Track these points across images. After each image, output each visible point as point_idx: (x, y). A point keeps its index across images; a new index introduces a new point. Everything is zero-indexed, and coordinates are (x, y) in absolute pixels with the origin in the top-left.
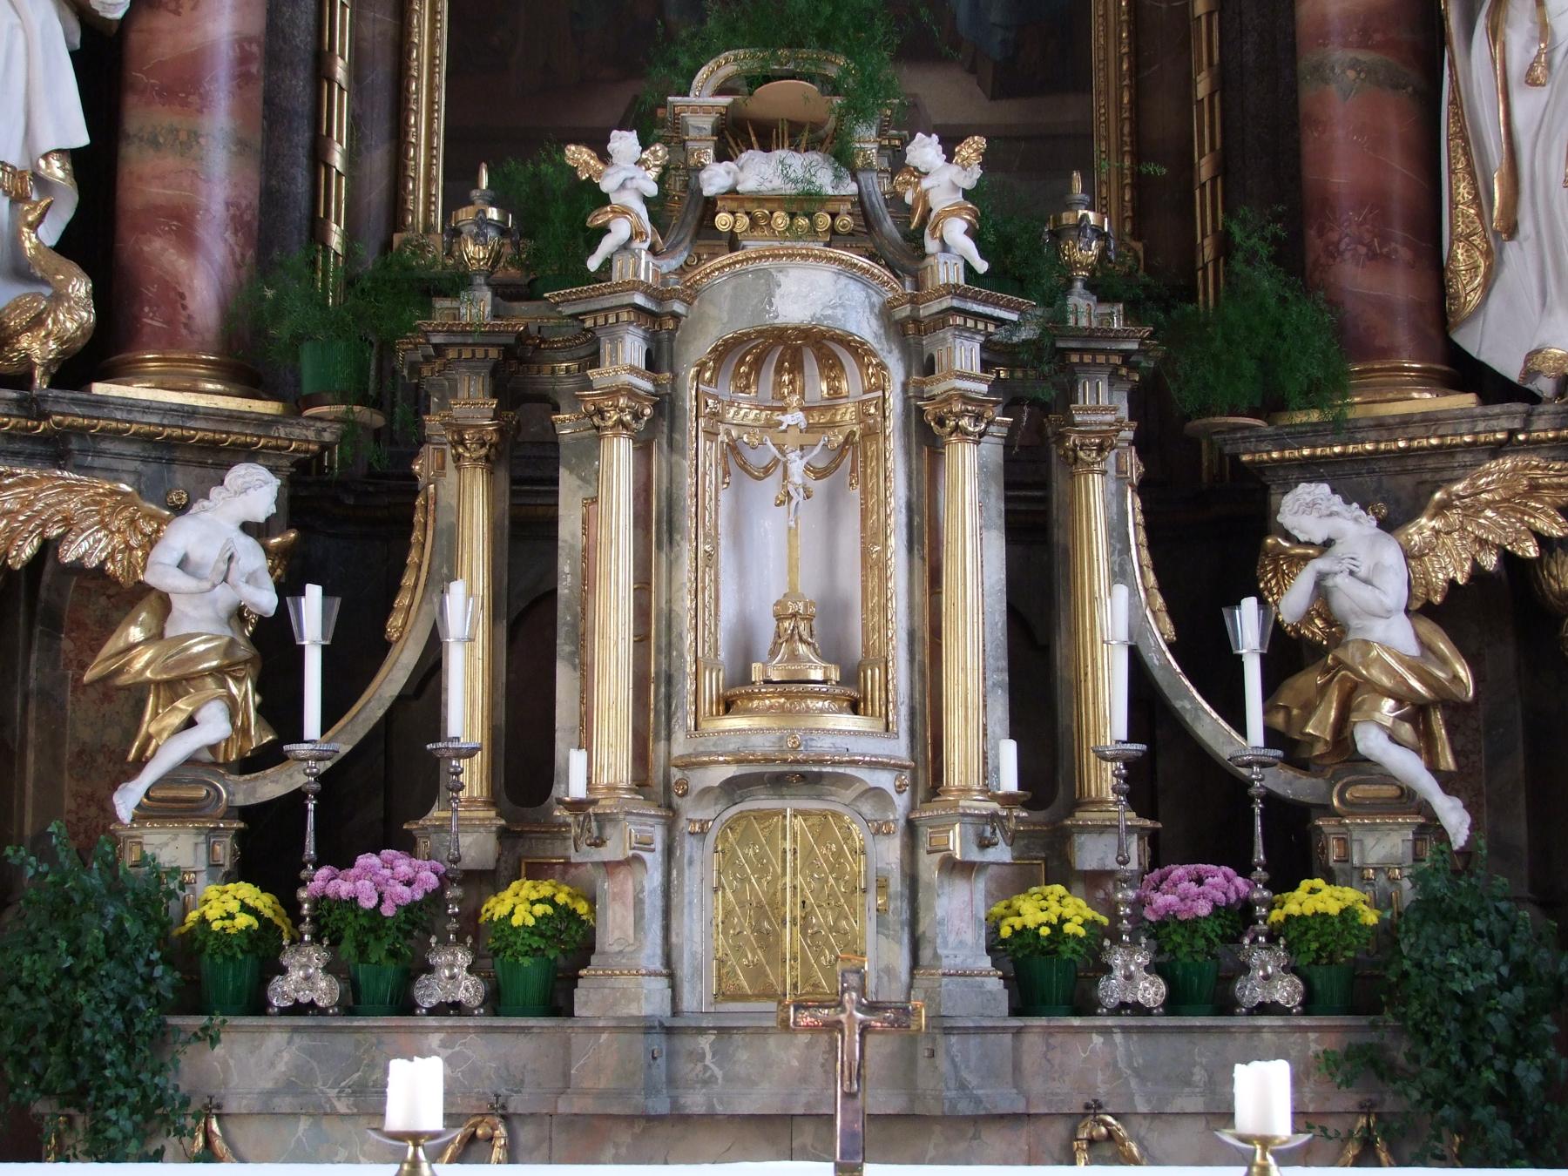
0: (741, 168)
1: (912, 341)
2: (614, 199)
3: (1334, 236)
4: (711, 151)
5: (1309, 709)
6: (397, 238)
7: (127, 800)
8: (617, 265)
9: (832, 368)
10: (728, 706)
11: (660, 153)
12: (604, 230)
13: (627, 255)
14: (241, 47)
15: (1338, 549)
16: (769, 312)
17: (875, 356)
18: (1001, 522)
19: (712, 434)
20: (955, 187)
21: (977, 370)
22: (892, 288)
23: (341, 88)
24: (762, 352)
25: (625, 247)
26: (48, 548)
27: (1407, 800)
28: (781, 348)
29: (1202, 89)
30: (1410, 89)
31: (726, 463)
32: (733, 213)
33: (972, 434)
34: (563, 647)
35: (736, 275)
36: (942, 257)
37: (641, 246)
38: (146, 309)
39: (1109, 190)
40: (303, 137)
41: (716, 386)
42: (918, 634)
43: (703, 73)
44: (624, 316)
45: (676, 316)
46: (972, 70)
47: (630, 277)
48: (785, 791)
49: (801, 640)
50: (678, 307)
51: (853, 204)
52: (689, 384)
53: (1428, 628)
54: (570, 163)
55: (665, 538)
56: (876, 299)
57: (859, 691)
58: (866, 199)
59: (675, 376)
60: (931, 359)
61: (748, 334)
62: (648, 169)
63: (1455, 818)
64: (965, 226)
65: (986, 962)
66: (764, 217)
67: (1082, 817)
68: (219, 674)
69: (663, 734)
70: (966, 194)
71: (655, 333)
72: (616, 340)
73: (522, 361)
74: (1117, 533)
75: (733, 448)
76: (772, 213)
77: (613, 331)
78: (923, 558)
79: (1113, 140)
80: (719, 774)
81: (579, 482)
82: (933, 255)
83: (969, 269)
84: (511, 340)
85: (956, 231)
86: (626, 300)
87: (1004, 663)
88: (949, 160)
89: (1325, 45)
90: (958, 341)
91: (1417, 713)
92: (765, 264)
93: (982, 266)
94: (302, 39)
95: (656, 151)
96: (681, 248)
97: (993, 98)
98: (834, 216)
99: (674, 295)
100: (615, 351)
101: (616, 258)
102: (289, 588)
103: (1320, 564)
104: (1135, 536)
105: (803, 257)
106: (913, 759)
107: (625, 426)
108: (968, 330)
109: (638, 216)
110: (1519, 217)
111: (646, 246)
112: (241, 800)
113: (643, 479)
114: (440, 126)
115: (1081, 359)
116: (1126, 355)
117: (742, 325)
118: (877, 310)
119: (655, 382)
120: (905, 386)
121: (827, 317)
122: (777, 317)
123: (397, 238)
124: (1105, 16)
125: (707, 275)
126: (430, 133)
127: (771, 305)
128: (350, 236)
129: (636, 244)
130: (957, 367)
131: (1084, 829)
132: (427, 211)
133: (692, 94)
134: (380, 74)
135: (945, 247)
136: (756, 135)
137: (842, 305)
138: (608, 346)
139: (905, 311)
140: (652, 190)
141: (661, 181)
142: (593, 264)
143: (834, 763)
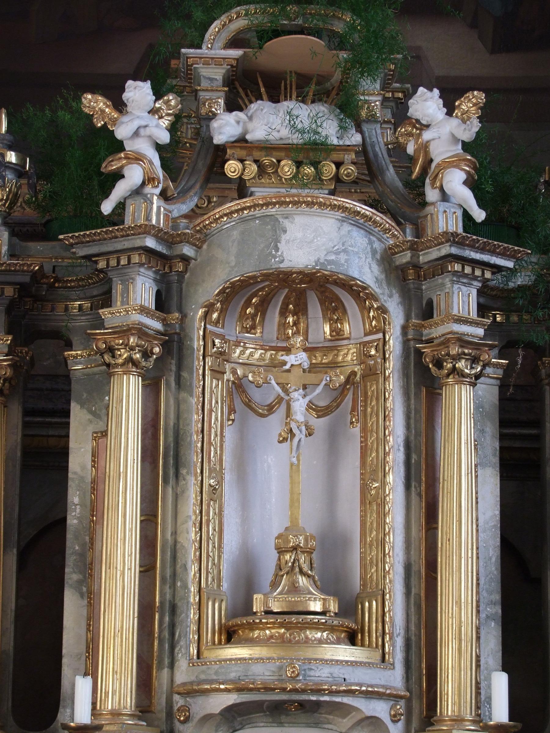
0: (250, 118)
1: (412, 286)
2: (128, 146)
4: (221, 101)
8: (130, 209)
9: (335, 310)
11: (173, 103)
12: (118, 176)
13: (139, 200)
16: (275, 257)
17: (376, 300)
18: (496, 460)
19: (218, 373)
20: (455, 139)
21: (474, 314)
22: (394, 236)
24: (268, 294)
25: (138, 192)
28: (287, 290)
31: (232, 400)
32: (242, 161)
33: (468, 376)
35: (243, 220)
36: (442, 206)
37: (152, 191)
41: (223, 327)
42: (414, 568)
43: (215, 27)
44: (136, 259)
45: (185, 259)
46: (473, 25)
47: (142, 221)
48: (283, 718)
49: (302, 572)
50: (188, 250)
51: (357, 153)
52: (197, 324)
54: (86, 110)
55: (171, 472)
57: (356, 622)
58: (369, 148)
59: (184, 316)
60: (430, 303)
61: (254, 277)
62: (161, 117)
66: (272, 165)
69: (166, 661)
70: (466, 146)
71: (164, 275)
72: (127, 282)
73: (37, 298)
76: (279, 161)
78: (420, 495)
81: (90, 417)
82: (433, 204)
83: (467, 217)
84: (27, 279)
86: (138, 243)
87: (497, 597)
88: (449, 113)
90: (456, 286)
92: (272, 211)
93: (479, 215)
95: (169, 101)
96: (191, 194)
97: (493, 52)
98: (338, 165)
99: (184, 239)
100: (126, 291)
101: (128, 202)
105: (308, 204)
106: (408, 689)
107: (135, 363)
108: (466, 276)
109: (151, 162)
111: (158, 191)
113: (151, 415)
118: (378, 256)
119: (164, 321)
120: (405, 329)
121: (330, 262)
122: (282, 261)
125: (216, 220)
127: (277, 250)
129: (149, 189)
130: (455, 312)
133: (204, 47)
135: (445, 197)
136: (265, 86)
137: (345, 251)
138: (120, 287)
139: (405, 257)
140: (165, 138)
141: (173, 129)
142: (107, 207)
143: (331, 693)
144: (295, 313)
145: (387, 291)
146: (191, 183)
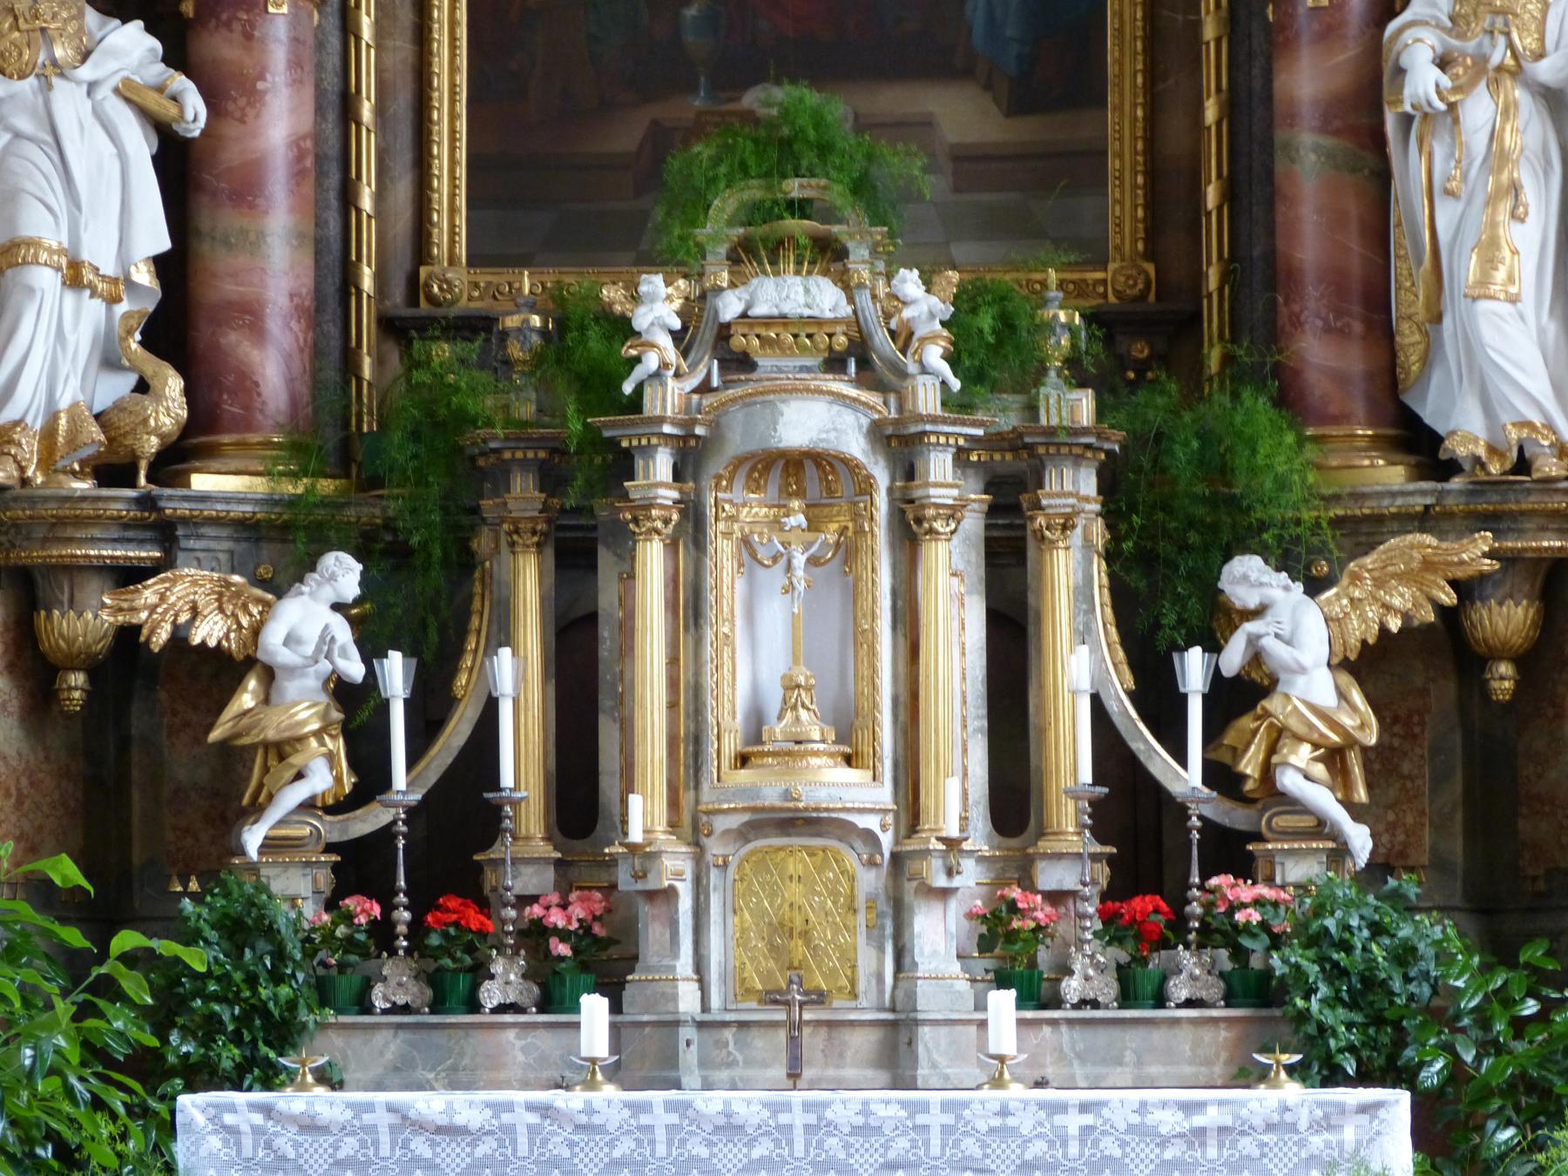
3: (1296, 308)
5: (1237, 753)
6: (424, 271)
7: (253, 838)
8: (648, 391)
10: (743, 760)
13: (656, 382)
14: (298, 146)
15: (1269, 618)
18: (982, 588)
19: (727, 535)
23: (368, 131)
26: (179, 639)
27: (1321, 828)
29: (1211, 113)
30: (1366, 172)
31: (740, 555)
33: (946, 534)
34: (605, 702)
36: (921, 379)
38: (225, 397)
39: (1122, 209)
40: (334, 180)
42: (902, 699)
44: (654, 441)
46: (988, 86)
48: (791, 830)
49: (803, 706)
51: (848, 324)
53: (1346, 679)
55: (691, 621)
56: (865, 422)
57: (850, 746)
58: (860, 313)
63: (1360, 839)
64: (940, 351)
65: (956, 967)
67: (1045, 846)
68: (317, 734)
69: (692, 784)
74: (1083, 593)
75: (746, 541)
77: (649, 451)
78: (905, 636)
79: (1127, 157)
80: (734, 821)
81: (615, 559)
85: (934, 355)
87: (984, 711)
89: (1291, 126)
91: (1334, 758)
93: (956, 384)
94: (332, 82)
98: (830, 336)
100: (647, 467)
102: (371, 651)
103: (1250, 627)
104: (1101, 596)
106: (896, 803)
107: (658, 532)
110: (1442, 307)
112: (335, 837)
113: (671, 571)
114: (462, 155)
115: (1047, 450)
116: (1088, 446)
117: (753, 446)
118: (864, 430)
120: (890, 490)
121: (822, 440)
123: (423, 271)
124: (1120, 31)
126: (453, 162)
127: (776, 431)
128: (379, 277)
131: (1045, 856)
132: (452, 242)
134: (402, 103)
135: (924, 370)
137: (835, 429)
140: (677, 324)
142: (628, 388)
143: (827, 810)
144: (796, 475)
145: (873, 460)
146: (699, 355)
